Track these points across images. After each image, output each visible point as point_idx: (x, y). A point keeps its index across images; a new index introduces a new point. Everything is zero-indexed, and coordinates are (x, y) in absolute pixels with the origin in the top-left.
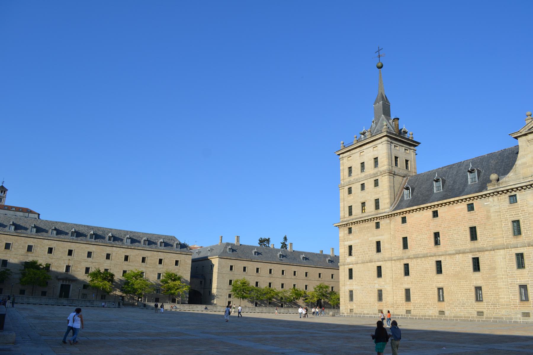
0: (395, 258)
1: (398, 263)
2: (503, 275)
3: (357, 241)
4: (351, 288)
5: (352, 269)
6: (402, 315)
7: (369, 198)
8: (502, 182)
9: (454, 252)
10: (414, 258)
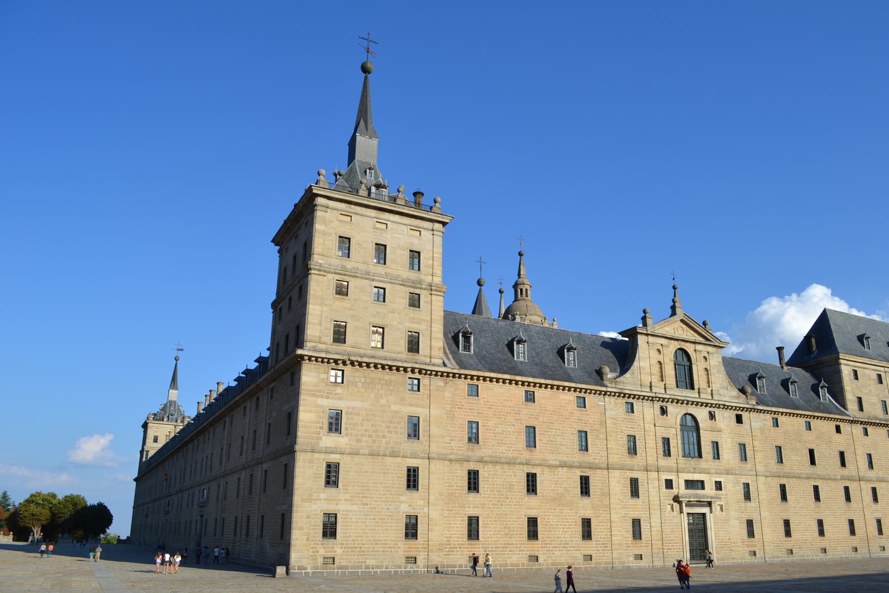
0: (453, 457)
1: (457, 466)
2: (617, 504)
3: (358, 404)
4: (331, 508)
5: (337, 465)
6: (460, 566)
7: (395, 323)
8: (620, 382)
9: (557, 463)
10: (491, 462)
